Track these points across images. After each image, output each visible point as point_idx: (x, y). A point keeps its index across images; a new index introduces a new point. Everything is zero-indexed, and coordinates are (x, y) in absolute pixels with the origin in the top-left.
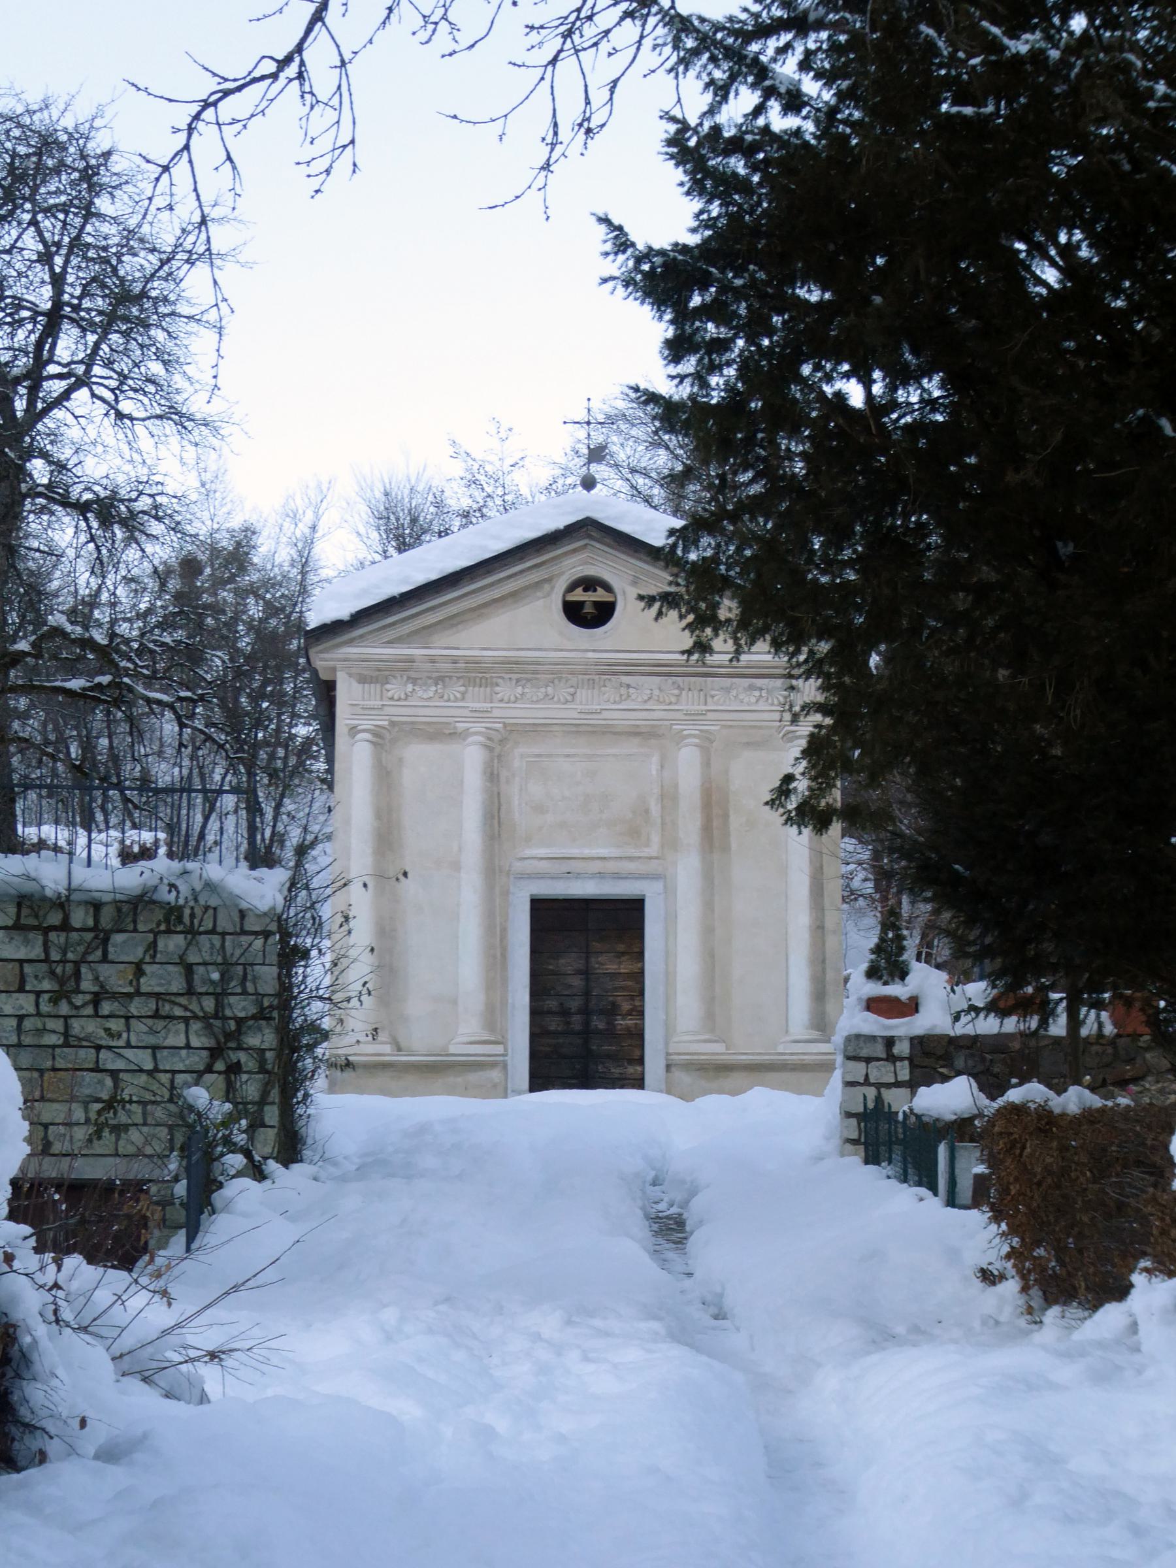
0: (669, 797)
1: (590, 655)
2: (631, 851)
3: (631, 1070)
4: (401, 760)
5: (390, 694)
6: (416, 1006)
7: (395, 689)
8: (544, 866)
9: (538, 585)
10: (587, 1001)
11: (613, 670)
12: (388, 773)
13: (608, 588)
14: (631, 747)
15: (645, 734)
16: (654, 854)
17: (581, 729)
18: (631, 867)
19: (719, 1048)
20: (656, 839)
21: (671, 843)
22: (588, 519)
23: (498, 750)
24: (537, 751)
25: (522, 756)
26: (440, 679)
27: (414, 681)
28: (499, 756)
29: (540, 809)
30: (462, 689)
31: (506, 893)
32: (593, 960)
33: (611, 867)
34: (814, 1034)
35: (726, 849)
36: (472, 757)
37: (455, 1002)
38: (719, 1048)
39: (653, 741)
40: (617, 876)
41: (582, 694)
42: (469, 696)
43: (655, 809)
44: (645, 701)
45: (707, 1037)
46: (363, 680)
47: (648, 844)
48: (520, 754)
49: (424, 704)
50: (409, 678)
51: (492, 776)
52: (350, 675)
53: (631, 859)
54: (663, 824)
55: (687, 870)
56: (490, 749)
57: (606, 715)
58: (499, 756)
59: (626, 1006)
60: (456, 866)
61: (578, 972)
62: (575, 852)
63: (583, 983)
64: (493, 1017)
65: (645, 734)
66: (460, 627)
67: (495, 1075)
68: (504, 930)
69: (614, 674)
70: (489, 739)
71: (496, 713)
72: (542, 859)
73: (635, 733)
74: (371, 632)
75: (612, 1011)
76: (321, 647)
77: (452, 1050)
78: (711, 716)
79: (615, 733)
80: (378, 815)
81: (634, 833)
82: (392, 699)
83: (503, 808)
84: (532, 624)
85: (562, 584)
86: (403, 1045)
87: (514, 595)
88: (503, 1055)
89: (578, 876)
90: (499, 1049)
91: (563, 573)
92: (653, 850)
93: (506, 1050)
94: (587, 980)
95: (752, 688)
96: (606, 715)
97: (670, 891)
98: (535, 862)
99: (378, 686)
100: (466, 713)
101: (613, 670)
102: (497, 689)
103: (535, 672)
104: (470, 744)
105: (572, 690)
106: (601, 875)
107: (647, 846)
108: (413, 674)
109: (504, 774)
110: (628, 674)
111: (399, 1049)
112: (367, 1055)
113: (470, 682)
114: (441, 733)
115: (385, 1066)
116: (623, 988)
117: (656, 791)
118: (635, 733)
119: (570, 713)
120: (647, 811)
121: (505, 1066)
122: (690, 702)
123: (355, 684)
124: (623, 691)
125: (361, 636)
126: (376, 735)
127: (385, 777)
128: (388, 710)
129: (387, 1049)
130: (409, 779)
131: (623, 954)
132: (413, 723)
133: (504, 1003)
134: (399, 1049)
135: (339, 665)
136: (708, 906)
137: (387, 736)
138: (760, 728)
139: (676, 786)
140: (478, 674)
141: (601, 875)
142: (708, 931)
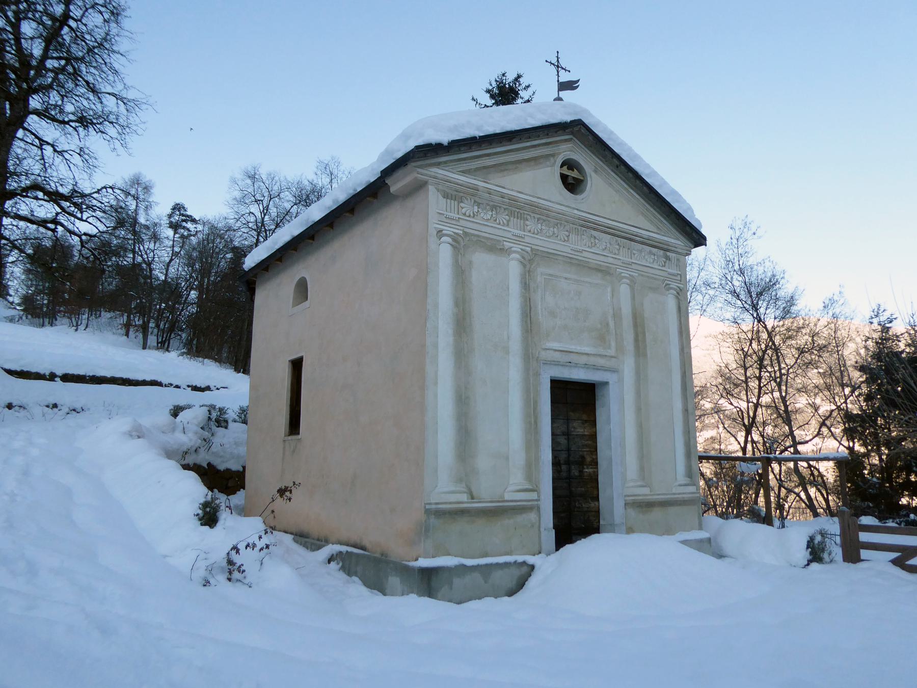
0: (617, 316)
1: (576, 212)
2: (601, 351)
3: (592, 505)
4: (471, 262)
5: (464, 211)
6: (483, 462)
7: (467, 207)
8: (557, 356)
9: (547, 157)
10: (569, 455)
11: (588, 225)
12: (463, 272)
13: (580, 169)
14: (596, 279)
15: (604, 271)
16: (613, 354)
17: (574, 261)
18: (601, 362)
19: (646, 491)
20: (613, 344)
21: (620, 348)
22: (580, 120)
23: (528, 266)
24: (551, 272)
25: (542, 274)
26: (494, 208)
27: (479, 205)
28: (529, 271)
29: (553, 314)
30: (507, 217)
31: (537, 374)
32: (571, 425)
33: (592, 360)
34: (687, 481)
35: (645, 355)
36: (514, 268)
37: (507, 458)
38: (646, 491)
39: (608, 277)
40: (595, 368)
41: (573, 237)
42: (511, 223)
43: (612, 324)
44: (604, 250)
45: (639, 483)
46: (446, 196)
47: (610, 348)
48: (542, 271)
49: (486, 224)
50: (475, 202)
51: (526, 286)
52: (438, 190)
53: (600, 356)
54: (616, 334)
55: (628, 366)
56: (524, 266)
57: (585, 254)
58: (529, 271)
59: (588, 459)
60: (506, 350)
61: (563, 434)
62: (572, 348)
63: (566, 441)
64: (531, 468)
65: (604, 271)
66: (505, 173)
67: (533, 516)
68: (536, 403)
69: (588, 228)
70: (523, 258)
71: (527, 240)
72: (556, 350)
73: (598, 270)
74: (452, 161)
75: (581, 462)
76: (419, 163)
77: (507, 497)
78: (634, 266)
79: (589, 268)
80: (457, 304)
81: (602, 339)
82: (465, 214)
83: (533, 310)
84: (538, 182)
85: (559, 161)
86: (475, 494)
87: (535, 159)
88: (537, 500)
89: (576, 365)
90: (534, 496)
91: (560, 153)
92: (612, 352)
93: (539, 496)
94: (568, 439)
95: (650, 253)
96: (585, 254)
97: (621, 381)
98: (551, 352)
99: (456, 203)
100: (509, 235)
101: (588, 225)
102: (527, 223)
103: (548, 216)
104: (512, 259)
105: (567, 233)
106: (586, 366)
107: (610, 348)
108: (477, 199)
109: (532, 285)
110: (595, 229)
111: (473, 498)
112: (450, 503)
113: (512, 214)
114: (495, 247)
115: (462, 512)
116: (587, 446)
117: (611, 311)
118: (598, 270)
119: (565, 248)
120: (608, 324)
121: (538, 508)
122: (624, 256)
123: (441, 197)
124: (592, 240)
125: (445, 162)
126: (454, 240)
127: (461, 275)
128: (462, 223)
129: (464, 497)
130: (477, 277)
131: (586, 421)
132: (478, 236)
133: (537, 459)
134: (473, 498)
135: (431, 180)
136: (638, 393)
137: (462, 244)
138: (655, 279)
139: (620, 309)
140: (518, 209)
141: (586, 366)
142: (638, 410)
